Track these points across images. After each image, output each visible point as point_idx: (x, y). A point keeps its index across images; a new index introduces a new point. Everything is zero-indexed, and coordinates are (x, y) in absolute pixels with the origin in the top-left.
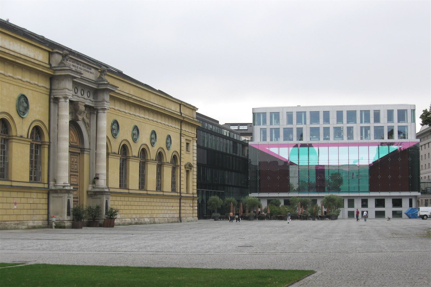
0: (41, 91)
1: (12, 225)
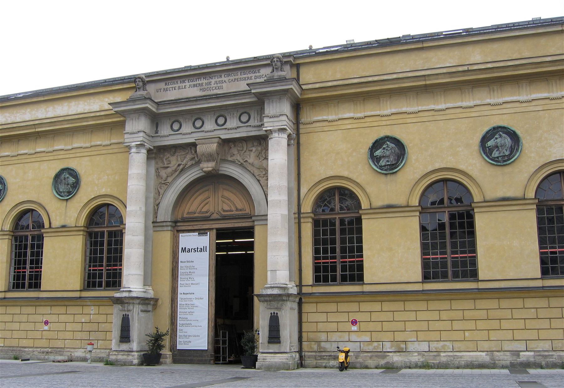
0: (111, 151)
1: (36, 353)
